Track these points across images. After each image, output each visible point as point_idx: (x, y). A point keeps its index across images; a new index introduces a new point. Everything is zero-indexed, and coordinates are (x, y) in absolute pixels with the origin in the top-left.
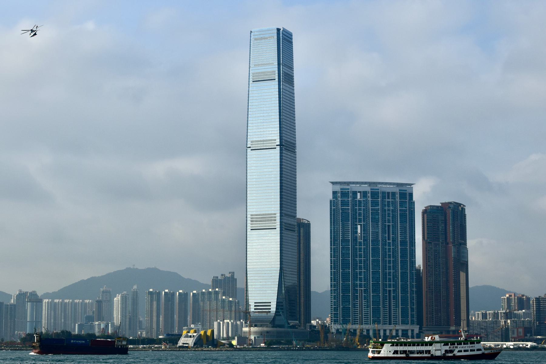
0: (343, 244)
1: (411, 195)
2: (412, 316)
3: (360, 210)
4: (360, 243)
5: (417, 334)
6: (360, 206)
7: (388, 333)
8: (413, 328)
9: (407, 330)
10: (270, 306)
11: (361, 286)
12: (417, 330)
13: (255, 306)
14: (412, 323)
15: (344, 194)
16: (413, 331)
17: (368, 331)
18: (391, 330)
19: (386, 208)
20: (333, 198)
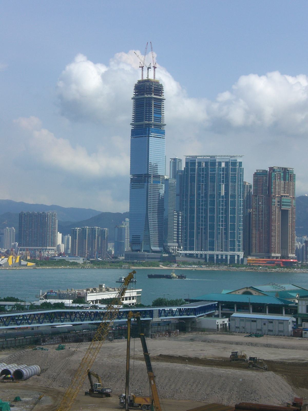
0: (191, 197)
1: (240, 163)
2: (239, 246)
3: (203, 174)
4: (202, 197)
5: (241, 259)
6: (203, 171)
7: (220, 257)
8: (239, 254)
9: (234, 255)
10: (140, 238)
11: (202, 225)
12: (241, 257)
13: (133, 238)
14: (239, 250)
15: (193, 163)
16: (238, 256)
17: (205, 255)
18: (222, 255)
19: (221, 173)
20: (186, 167)
